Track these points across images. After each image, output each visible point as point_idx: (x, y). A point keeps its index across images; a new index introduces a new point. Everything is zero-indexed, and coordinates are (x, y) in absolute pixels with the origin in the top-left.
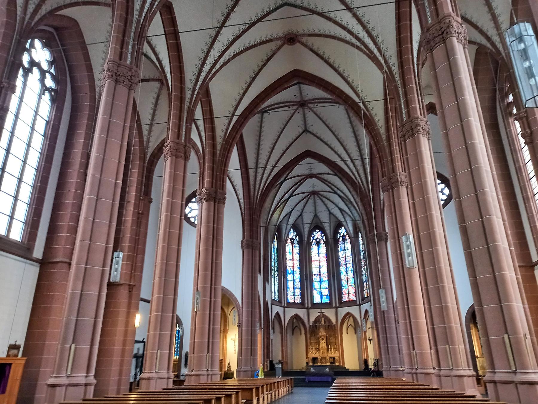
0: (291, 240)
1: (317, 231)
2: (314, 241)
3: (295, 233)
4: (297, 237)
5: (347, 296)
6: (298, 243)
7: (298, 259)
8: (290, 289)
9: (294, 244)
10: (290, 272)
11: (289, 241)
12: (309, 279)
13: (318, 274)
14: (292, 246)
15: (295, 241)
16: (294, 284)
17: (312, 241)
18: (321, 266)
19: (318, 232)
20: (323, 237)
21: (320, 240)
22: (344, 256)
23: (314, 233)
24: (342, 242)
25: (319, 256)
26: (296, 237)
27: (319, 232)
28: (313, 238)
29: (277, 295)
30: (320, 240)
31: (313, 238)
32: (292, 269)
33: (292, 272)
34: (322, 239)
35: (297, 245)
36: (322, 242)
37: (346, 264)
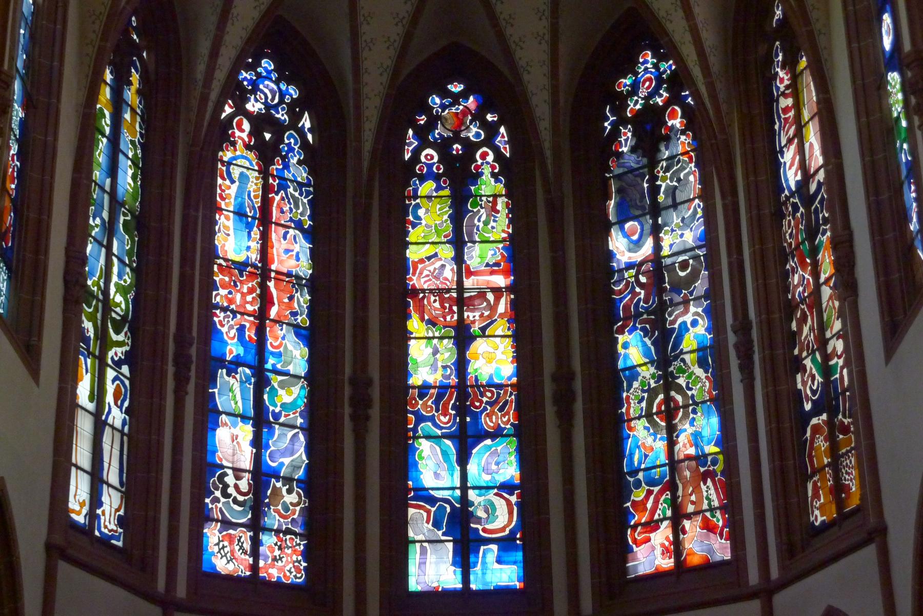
0: (256, 132)
1: (456, 88)
2: (430, 155)
3: (293, 92)
4: (306, 122)
5: (662, 535)
6: (311, 158)
7: (304, 268)
8: (230, 479)
9: (276, 168)
10: (233, 349)
11: (243, 132)
12: (375, 412)
13: (443, 388)
14: (264, 173)
15: (290, 139)
16: (258, 443)
17: (417, 153)
18: (475, 329)
19: (456, 99)
20: (491, 130)
21: (470, 147)
22: (648, 248)
23: (435, 101)
24: (632, 161)
25: (459, 259)
26: (295, 117)
27: (464, 95)
28: (422, 134)
29: (111, 502)
30: (470, 147)
31: (422, 134)
32: (250, 333)
33: (251, 358)
34: (489, 141)
35: (302, 174)
36: (485, 161)
37: (661, 310)
